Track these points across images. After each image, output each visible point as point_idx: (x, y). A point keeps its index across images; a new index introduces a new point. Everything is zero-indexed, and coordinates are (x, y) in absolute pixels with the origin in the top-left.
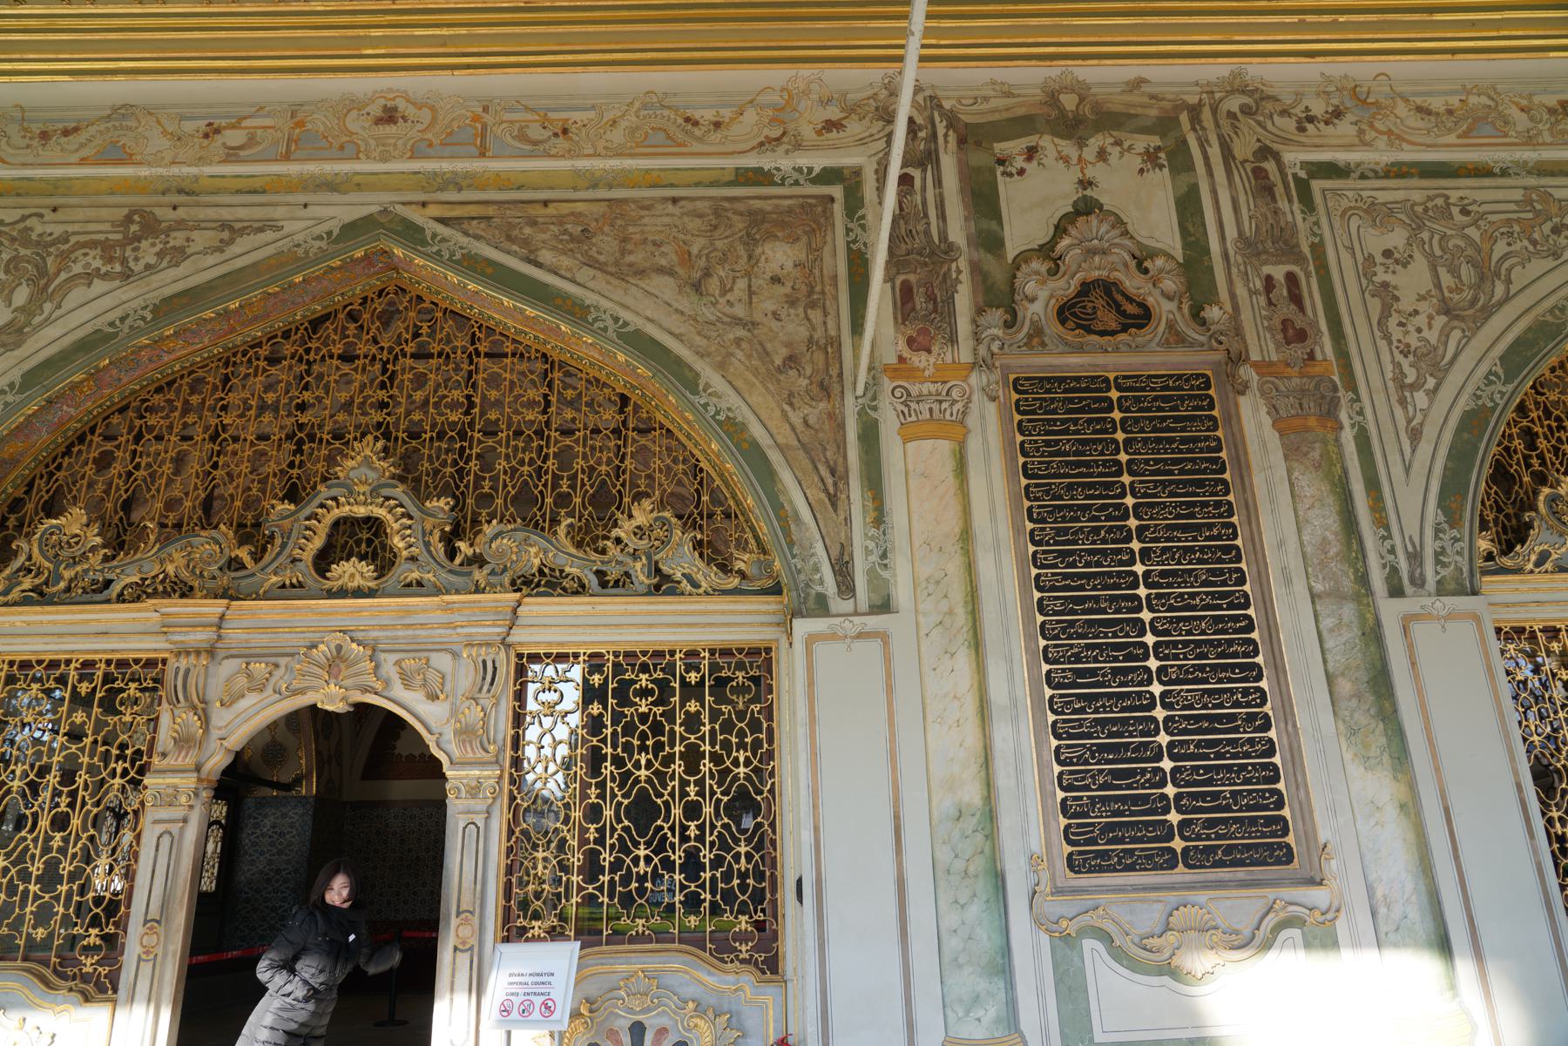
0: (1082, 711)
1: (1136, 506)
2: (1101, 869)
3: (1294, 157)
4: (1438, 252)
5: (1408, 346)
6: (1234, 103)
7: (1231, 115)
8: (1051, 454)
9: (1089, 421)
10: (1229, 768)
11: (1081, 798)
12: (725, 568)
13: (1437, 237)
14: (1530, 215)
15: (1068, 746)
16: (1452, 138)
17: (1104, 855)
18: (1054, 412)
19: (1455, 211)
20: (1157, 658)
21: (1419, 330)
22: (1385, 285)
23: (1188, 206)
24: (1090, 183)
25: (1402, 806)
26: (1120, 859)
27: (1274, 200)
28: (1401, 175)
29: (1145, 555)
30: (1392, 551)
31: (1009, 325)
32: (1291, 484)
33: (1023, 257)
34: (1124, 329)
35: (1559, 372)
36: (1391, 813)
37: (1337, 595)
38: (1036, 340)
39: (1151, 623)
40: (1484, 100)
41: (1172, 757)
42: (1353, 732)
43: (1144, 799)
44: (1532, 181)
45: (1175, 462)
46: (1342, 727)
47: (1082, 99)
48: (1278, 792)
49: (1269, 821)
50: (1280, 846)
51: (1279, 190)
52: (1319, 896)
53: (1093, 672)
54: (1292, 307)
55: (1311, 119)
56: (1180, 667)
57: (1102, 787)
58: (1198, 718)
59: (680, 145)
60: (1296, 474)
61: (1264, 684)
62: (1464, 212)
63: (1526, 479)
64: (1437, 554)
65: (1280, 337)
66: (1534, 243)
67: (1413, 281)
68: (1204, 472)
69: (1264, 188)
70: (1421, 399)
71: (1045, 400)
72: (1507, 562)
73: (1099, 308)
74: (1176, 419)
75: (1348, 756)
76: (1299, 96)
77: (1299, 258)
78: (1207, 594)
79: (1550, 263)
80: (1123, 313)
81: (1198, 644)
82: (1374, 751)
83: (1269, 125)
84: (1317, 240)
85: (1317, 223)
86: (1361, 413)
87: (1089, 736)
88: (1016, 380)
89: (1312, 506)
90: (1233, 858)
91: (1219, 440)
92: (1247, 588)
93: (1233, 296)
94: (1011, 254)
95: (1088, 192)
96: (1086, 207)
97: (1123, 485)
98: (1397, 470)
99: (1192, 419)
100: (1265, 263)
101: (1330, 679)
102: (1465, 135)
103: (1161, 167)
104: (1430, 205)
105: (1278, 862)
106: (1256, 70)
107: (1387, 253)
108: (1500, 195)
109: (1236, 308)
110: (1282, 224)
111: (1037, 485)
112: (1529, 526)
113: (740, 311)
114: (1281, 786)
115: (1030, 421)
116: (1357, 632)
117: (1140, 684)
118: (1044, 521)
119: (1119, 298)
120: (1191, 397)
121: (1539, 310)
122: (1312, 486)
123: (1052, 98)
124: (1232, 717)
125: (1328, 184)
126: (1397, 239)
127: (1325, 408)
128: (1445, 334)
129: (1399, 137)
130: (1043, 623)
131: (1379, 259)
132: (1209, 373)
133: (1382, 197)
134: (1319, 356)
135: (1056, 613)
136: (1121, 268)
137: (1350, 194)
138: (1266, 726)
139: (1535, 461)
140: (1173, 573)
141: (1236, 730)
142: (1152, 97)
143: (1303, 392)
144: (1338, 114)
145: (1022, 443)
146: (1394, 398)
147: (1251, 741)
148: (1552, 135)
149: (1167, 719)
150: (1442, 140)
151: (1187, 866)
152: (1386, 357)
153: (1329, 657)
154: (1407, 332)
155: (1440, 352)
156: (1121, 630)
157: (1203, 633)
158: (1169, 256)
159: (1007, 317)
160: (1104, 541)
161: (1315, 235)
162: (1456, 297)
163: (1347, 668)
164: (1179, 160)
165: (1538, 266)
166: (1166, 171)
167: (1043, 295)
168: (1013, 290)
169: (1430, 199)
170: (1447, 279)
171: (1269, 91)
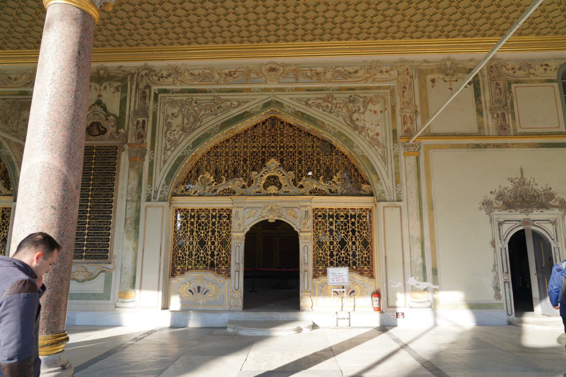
3: (155, 88)
6: (143, 73)
7: (142, 76)
10: (99, 238)
12: (9, 189)
16: (197, 82)
19: (193, 102)
22: (170, 123)
23: (123, 102)
25: (134, 248)
27: (145, 100)
28: (182, 92)
29: (92, 189)
30: (151, 191)
34: (99, 135)
36: (131, 250)
37: (132, 201)
40: (209, 71)
41: (88, 235)
42: (127, 232)
44: (216, 94)
45: (105, 168)
47: (105, 72)
49: (105, 250)
51: (148, 97)
52: (110, 266)
55: (162, 77)
59: (6, 85)
62: (196, 103)
66: (211, 111)
67: (176, 122)
69: (144, 97)
72: (187, 193)
74: (108, 157)
75: (125, 237)
76: (161, 70)
77: (147, 116)
79: (214, 117)
80: (100, 130)
81: (99, 211)
82: (131, 236)
83: (151, 79)
85: (157, 106)
86: (153, 156)
93: (128, 126)
95: (100, 98)
96: (99, 103)
98: (158, 171)
100: (139, 117)
103: (119, 91)
105: (105, 259)
106: (150, 63)
107: (172, 114)
108: (207, 98)
109: (128, 129)
113: (15, 128)
116: (135, 209)
119: (100, 126)
121: (207, 130)
122: (133, 174)
123: (98, 71)
124: (103, 227)
125: (163, 95)
126: (176, 110)
128: (180, 136)
129: (184, 82)
131: (170, 116)
133: (176, 98)
134: (145, 142)
138: (109, 230)
140: (98, 194)
142: (123, 71)
144: (169, 75)
147: (105, 233)
150: (194, 83)
152: (164, 142)
158: (114, 116)
164: (124, 89)
169: (188, 99)
170: (186, 121)
171: (154, 69)
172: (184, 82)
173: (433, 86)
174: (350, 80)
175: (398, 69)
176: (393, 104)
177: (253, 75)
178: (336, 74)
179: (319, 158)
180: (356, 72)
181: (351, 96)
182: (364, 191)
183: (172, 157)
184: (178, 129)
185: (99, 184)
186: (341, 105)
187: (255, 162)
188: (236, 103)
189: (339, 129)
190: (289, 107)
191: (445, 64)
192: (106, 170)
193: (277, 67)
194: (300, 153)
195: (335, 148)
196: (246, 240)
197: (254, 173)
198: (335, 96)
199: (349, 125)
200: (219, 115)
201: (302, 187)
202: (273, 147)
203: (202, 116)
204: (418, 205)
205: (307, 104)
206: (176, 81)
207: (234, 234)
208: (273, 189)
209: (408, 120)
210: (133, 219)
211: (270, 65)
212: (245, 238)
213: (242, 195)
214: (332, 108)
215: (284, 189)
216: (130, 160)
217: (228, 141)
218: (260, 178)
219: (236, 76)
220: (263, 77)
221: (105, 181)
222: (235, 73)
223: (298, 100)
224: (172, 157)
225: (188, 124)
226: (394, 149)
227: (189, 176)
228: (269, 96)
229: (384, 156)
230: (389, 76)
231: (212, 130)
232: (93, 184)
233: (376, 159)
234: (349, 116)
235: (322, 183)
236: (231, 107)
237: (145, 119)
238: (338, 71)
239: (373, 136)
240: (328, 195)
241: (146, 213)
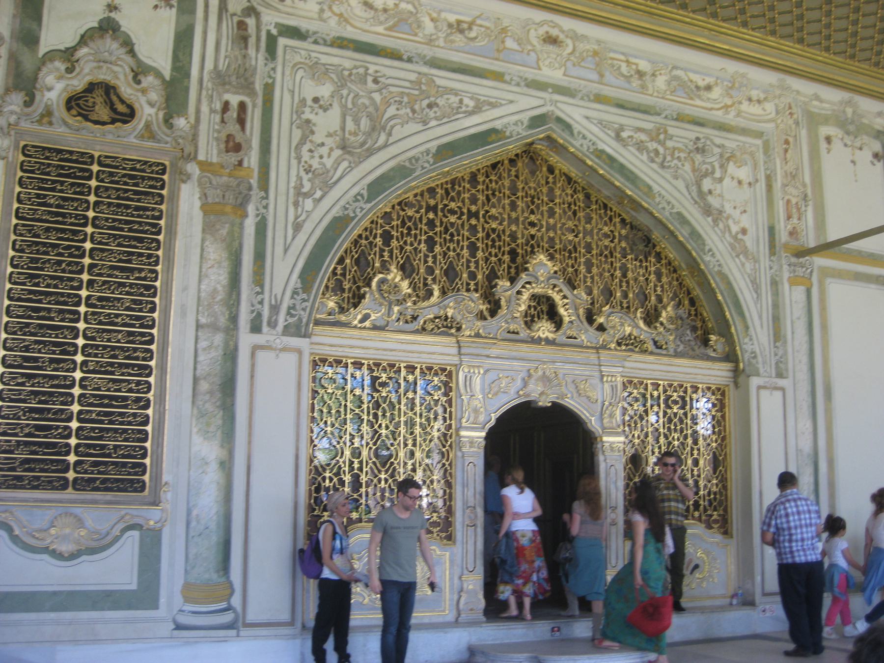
0: (22, 384)
1: (92, 250)
2: (15, 487)
3: (270, 19)
4: (350, 106)
5: (311, 166)
8: (39, 204)
9: (73, 184)
10: (116, 431)
11: (10, 441)
13: (352, 95)
14: (416, 92)
15: (9, 407)
16: (380, 29)
17: (19, 478)
18: (48, 174)
19: (370, 79)
20: (83, 355)
21: (321, 157)
22: (308, 121)
23: (183, 40)
24: (116, 8)
25: (222, 464)
26: (30, 481)
27: (246, 47)
28: (341, 47)
29: (90, 283)
30: (261, 302)
31: (29, 103)
32: (202, 250)
33: (51, 56)
34: (113, 121)
35: (419, 198)
37: (213, 327)
38: (46, 120)
39: (84, 331)
40: (410, 7)
41: (79, 420)
42: (202, 415)
43: (55, 445)
44: (425, 69)
45: (127, 222)
46: (195, 411)
48: (145, 449)
49: (135, 465)
50: (138, 481)
51: (252, 41)
53: (36, 359)
54: (238, 127)
56: (97, 362)
57: (26, 436)
58: (102, 397)
60: (207, 243)
61: (152, 379)
62: (376, 81)
63: (377, 265)
64: (289, 308)
65: (223, 146)
66: (414, 111)
67: (327, 123)
68: (145, 232)
69: (242, 38)
70: (308, 204)
71: (43, 164)
72: (343, 318)
73: (100, 102)
74: (136, 193)
75: (195, 430)
77: (252, 93)
78: (127, 316)
79: (420, 127)
80: (113, 109)
81: (113, 348)
82: (212, 429)
84: (270, 81)
85: (274, 69)
87: (24, 401)
88: (25, 146)
89: (212, 267)
90: (106, 486)
91: (161, 211)
92: (156, 315)
93: (198, 111)
94: (42, 50)
95: (113, 15)
96: (108, 27)
97: (86, 234)
98: (279, 249)
99: (146, 194)
100: (227, 91)
101: (196, 380)
102: (389, 29)
103: (171, 6)
104: (354, 71)
105: (135, 491)
107: (316, 100)
108: (402, 74)
109: (198, 120)
110: (247, 65)
111: (24, 225)
112: (363, 297)
114: (148, 445)
115: (29, 178)
116: (220, 352)
117: (67, 371)
118: (22, 251)
119: (114, 98)
120: (150, 178)
122: (216, 252)
124: (125, 399)
126: (325, 91)
127: (239, 201)
128: (337, 163)
129: (346, 20)
130: (8, 323)
131: (309, 102)
132: (167, 163)
133: (324, 59)
134: (245, 164)
135: (18, 317)
136: (122, 77)
137: (303, 52)
138: (147, 407)
139: (386, 254)
140: (107, 299)
141: (126, 407)
143: (228, 187)
145: (20, 193)
146: (291, 200)
147: (134, 415)
148: (445, 42)
149: (81, 396)
151: (75, 489)
152: (294, 172)
153: (199, 367)
154: (313, 157)
155: (331, 174)
156: (62, 333)
157: (118, 341)
158: (158, 74)
159: (27, 98)
160: (63, 271)
161: (270, 77)
162: (352, 138)
163: (209, 375)
166: (174, 10)
167: (59, 86)
168: (36, 79)
169: (356, 67)
170: (350, 125)
172: (346, 20)
173: (829, 151)
174: (698, 102)
175: (777, 101)
176: (768, 172)
177: (510, 43)
178: (674, 83)
180: (708, 88)
181: (698, 139)
184: (330, 142)
185: (112, 268)
186: (682, 155)
188: (472, 104)
189: (678, 208)
190: (584, 137)
191: (844, 112)
192: (130, 230)
193: (562, 37)
196: (486, 448)
198: (671, 131)
199: (696, 202)
200: (433, 123)
201: (601, 328)
204: (810, 389)
205: (618, 137)
206: (327, 14)
207: (463, 433)
208: (544, 329)
209: (794, 210)
210: (218, 380)
211: (545, 28)
212: (483, 443)
213: (478, 335)
214: (665, 158)
216: (207, 209)
218: (516, 300)
219: (473, 34)
220: (532, 54)
221: (129, 261)
222: (470, 29)
223: (601, 123)
225: (355, 134)
226: (771, 268)
228: (541, 102)
229: (755, 279)
230: (762, 112)
231: (417, 160)
232: (91, 266)
233: (742, 284)
235: (641, 324)
236: (457, 110)
237: (247, 99)
238: (676, 78)
239: (737, 233)
240: (652, 353)
241: (253, 366)
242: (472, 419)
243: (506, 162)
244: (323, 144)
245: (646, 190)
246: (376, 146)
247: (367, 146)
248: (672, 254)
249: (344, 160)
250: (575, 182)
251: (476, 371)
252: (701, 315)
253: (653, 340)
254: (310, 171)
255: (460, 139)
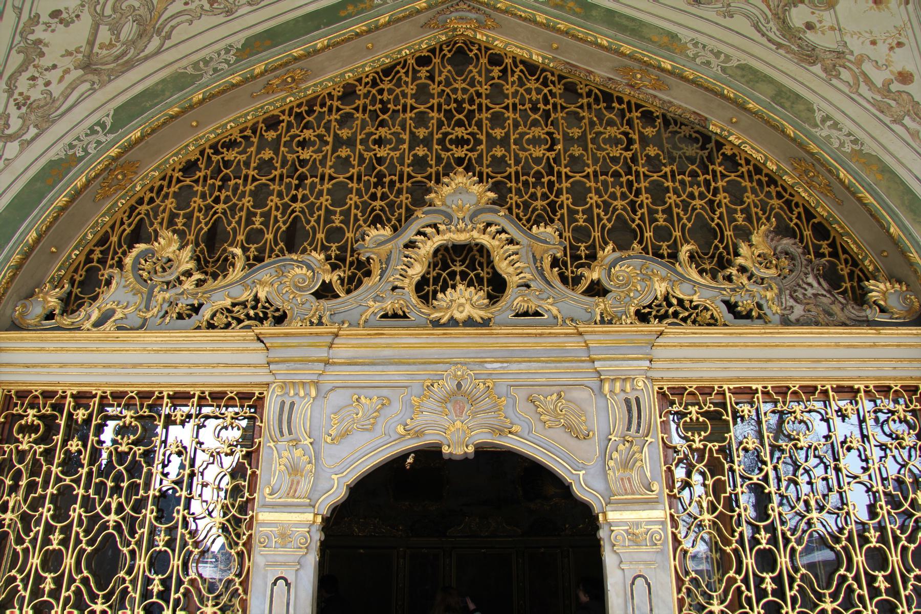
4: (108, 11)
21: (48, 84)
22: (40, 41)
35: (248, 133)
72: (67, 321)
79: (222, 18)
121: (184, 63)
128: (73, 87)
154: (34, 86)
155: (57, 105)
162: (105, 52)
165: (207, 21)
170: (104, 35)
179: (660, 184)
182: (883, 310)
183: (19, 166)
187: (384, 197)
189: (738, 59)
194: (576, 163)
195: (719, 145)
196: (324, 547)
197: (376, 234)
199: (779, 46)
201: (597, 290)
202: (460, 142)
203: (173, 17)
207: (264, 516)
212: (317, 536)
215: (514, 299)
217: (272, 123)
218: (400, 256)
224: (19, 166)
225: (111, 45)
227: (96, 255)
231: (207, 62)
234: (775, 15)
235: (694, 275)
239: (887, 84)
242: (285, 488)
243: (411, 61)
244: (55, 67)
245: (665, 40)
246: (142, 55)
247: (125, 58)
248: (755, 151)
249: (85, 81)
250: (543, 70)
251: (302, 393)
252: (845, 251)
253: (726, 303)
254: (24, 105)
255: (287, 22)
